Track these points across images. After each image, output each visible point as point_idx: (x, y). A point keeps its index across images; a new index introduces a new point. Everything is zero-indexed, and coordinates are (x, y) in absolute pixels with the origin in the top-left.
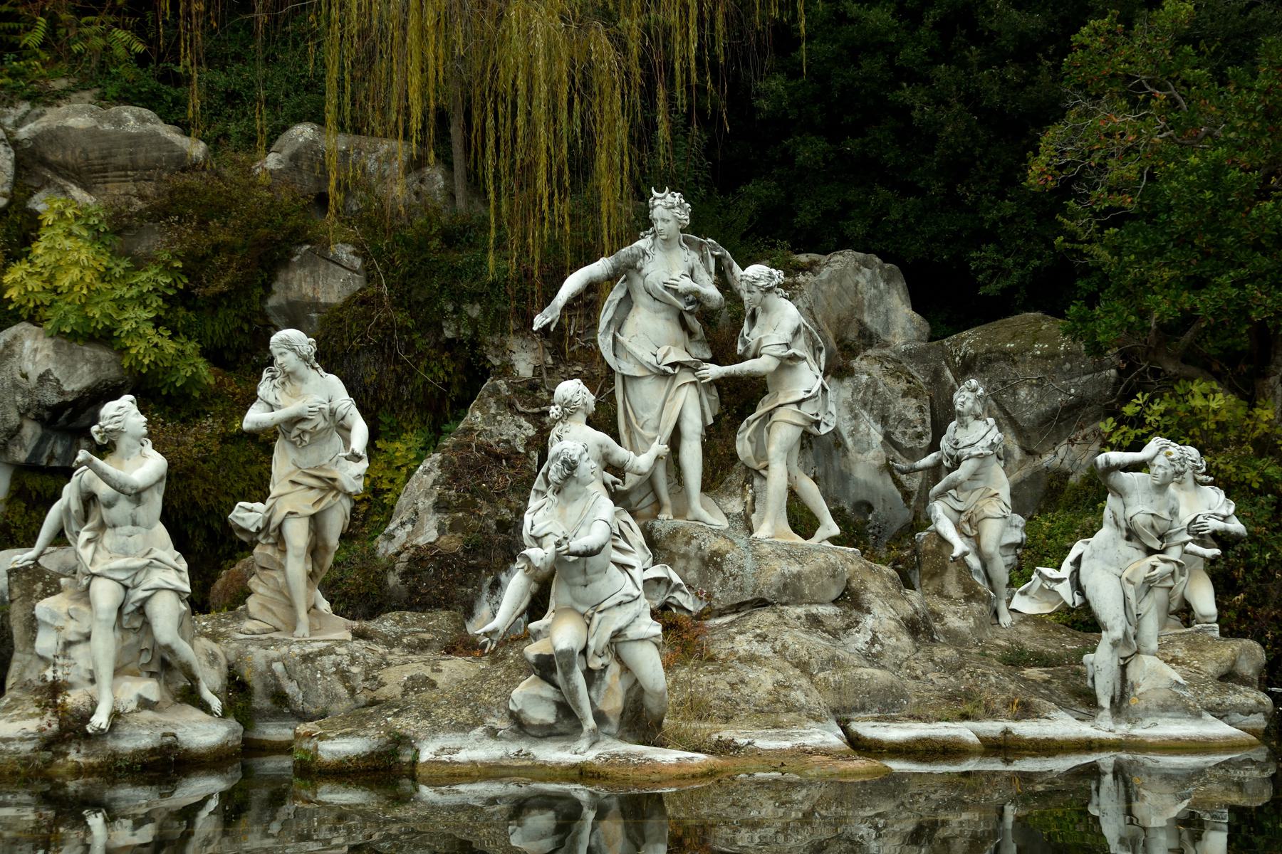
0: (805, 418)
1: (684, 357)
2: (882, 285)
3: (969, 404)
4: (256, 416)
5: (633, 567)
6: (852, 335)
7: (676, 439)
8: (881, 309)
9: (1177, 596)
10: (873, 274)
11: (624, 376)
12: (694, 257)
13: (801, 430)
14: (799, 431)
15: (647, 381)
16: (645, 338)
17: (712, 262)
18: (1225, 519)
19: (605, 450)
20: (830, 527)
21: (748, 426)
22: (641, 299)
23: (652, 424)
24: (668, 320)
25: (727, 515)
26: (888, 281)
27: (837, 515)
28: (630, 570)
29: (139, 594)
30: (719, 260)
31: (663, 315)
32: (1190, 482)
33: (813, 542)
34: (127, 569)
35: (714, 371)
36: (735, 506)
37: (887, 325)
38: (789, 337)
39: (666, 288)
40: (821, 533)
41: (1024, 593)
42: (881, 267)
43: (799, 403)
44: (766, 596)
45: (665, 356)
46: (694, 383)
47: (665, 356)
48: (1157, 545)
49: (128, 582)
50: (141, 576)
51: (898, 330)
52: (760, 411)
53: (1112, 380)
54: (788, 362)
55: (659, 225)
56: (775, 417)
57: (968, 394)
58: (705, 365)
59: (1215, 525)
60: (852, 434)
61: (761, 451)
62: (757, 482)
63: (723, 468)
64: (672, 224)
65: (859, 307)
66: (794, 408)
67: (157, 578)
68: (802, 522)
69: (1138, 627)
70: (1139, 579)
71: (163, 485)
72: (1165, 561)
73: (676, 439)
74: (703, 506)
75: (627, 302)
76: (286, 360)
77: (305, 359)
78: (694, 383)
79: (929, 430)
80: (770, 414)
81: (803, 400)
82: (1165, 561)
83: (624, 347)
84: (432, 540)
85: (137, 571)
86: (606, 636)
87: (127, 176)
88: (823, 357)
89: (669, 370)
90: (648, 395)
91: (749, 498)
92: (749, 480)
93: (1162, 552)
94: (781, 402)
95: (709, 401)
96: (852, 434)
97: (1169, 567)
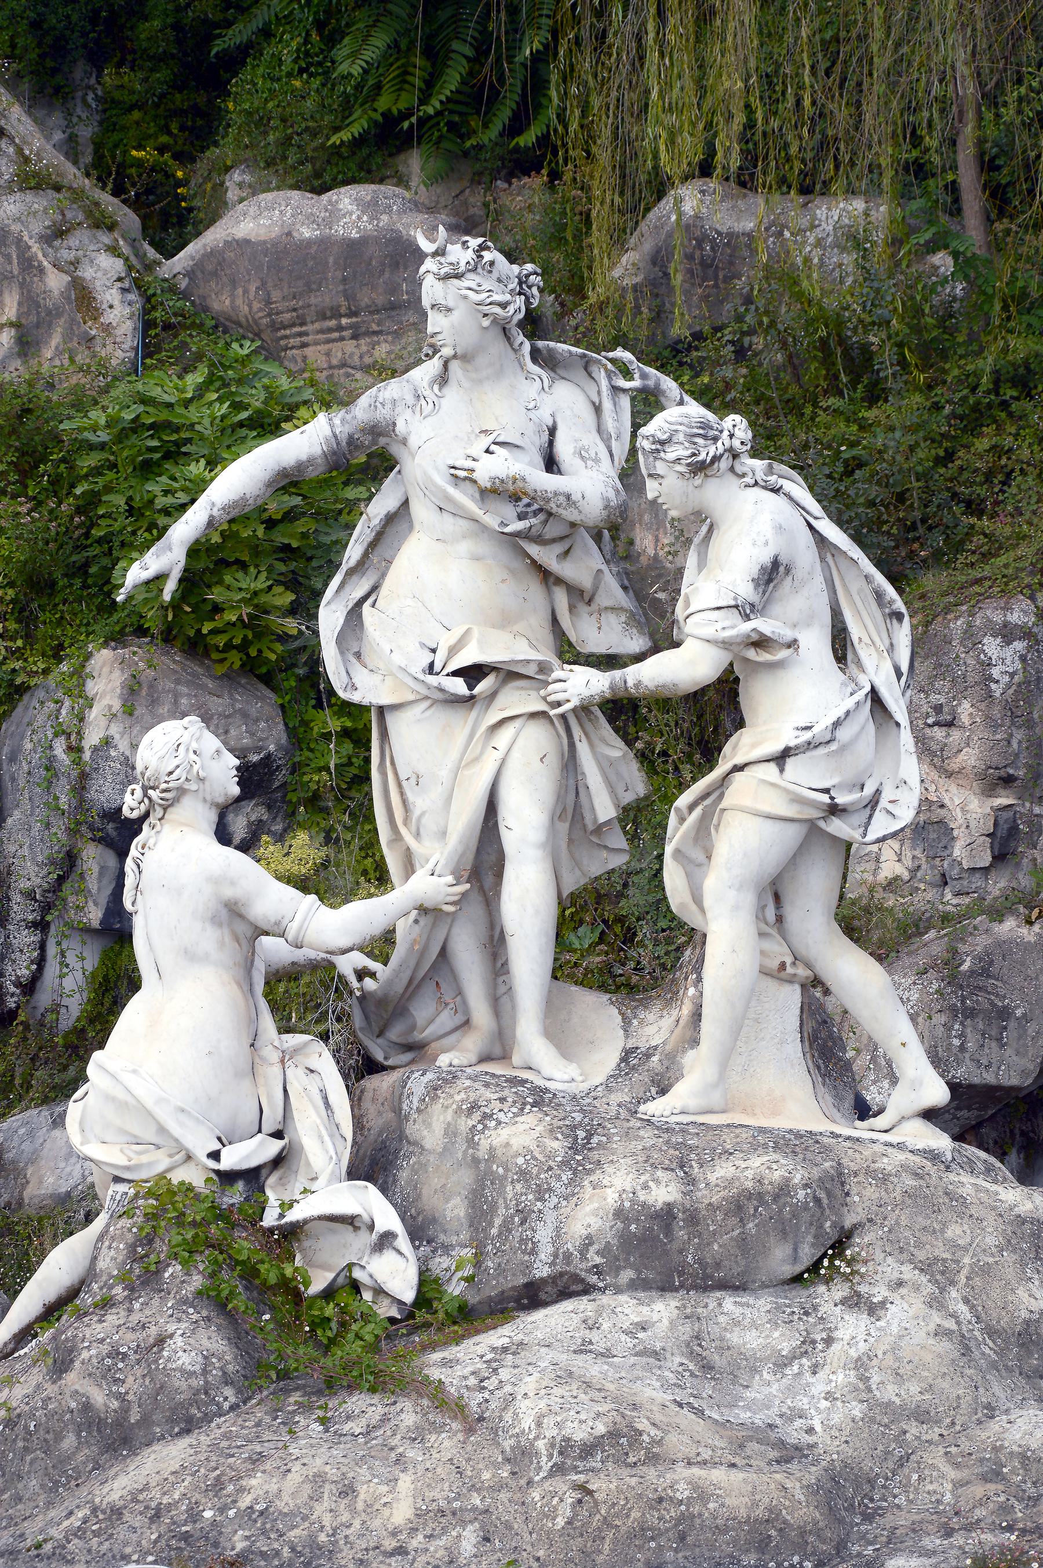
0: (798, 800)
7: (484, 863)
11: (381, 710)
14: (793, 834)
16: (413, 612)
19: (228, 893)
21: (682, 820)
24: (476, 558)
31: (465, 547)
35: (583, 683)
38: (746, 591)
43: (781, 758)
44: (579, 1267)
47: (453, 651)
54: (751, 654)
55: (435, 322)
63: (622, 939)
66: (772, 767)
73: (484, 863)
74: (557, 1031)
84: (74, 1110)
87: (340, 328)
89: (459, 686)
94: (739, 760)
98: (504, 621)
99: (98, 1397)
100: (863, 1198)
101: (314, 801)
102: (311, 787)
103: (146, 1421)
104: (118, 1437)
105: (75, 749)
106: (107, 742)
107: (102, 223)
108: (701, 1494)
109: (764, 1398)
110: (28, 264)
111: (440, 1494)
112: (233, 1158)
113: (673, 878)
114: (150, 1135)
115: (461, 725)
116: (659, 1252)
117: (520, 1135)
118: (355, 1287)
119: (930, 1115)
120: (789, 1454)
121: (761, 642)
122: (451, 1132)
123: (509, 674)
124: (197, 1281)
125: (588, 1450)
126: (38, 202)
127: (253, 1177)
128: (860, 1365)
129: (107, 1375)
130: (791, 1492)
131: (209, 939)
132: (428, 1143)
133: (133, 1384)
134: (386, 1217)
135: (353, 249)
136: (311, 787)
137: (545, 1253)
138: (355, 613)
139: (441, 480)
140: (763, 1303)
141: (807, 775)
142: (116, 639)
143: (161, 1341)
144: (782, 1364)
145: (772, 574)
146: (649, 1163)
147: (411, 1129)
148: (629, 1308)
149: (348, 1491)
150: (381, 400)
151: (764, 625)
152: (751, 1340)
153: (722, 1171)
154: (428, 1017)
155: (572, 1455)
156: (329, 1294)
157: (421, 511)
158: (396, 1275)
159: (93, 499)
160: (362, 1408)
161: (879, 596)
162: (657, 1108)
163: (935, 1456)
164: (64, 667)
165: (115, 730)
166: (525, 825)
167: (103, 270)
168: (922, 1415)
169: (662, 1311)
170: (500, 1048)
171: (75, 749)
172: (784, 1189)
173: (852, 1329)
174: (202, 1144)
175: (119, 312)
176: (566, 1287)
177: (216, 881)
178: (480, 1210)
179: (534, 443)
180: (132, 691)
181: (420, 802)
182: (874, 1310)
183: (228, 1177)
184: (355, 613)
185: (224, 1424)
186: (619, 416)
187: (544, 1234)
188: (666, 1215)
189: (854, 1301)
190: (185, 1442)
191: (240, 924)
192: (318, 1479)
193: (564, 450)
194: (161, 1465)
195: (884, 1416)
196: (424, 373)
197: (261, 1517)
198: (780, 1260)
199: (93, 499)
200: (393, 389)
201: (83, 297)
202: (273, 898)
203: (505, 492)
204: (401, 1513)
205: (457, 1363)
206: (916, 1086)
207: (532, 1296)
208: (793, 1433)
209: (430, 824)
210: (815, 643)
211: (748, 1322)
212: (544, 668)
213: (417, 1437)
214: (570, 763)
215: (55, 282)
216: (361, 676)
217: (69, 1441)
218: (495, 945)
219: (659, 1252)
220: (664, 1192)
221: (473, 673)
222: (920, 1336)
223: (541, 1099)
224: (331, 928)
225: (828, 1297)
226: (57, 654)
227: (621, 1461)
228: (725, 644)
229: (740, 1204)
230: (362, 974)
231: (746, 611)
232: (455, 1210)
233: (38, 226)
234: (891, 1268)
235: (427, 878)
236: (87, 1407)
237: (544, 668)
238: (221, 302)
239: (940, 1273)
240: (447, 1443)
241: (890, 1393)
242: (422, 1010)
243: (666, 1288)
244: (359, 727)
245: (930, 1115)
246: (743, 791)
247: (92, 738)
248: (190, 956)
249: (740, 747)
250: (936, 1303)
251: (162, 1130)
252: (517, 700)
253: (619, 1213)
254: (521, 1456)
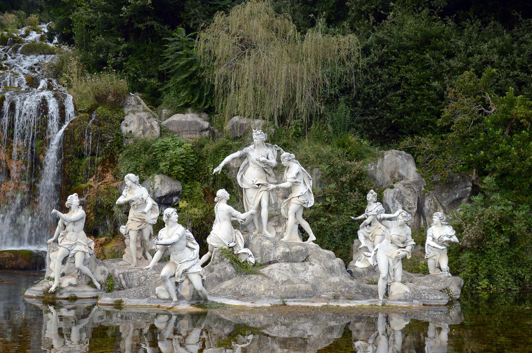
0: (301, 202)
2: (405, 161)
3: (371, 198)
4: (121, 200)
6: (396, 176)
7: (259, 207)
8: (406, 168)
9: (437, 262)
10: (402, 157)
14: (300, 206)
15: (249, 190)
18: (451, 237)
19: (230, 211)
20: (312, 237)
23: (252, 203)
26: (407, 160)
27: (316, 234)
29: (72, 252)
31: (257, 169)
32: (440, 224)
33: (307, 242)
34: (69, 245)
35: (272, 186)
37: (408, 173)
38: (295, 176)
40: (309, 239)
41: (359, 261)
42: (405, 156)
43: (298, 197)
44: (277, 259)
48: (401, 245)
49: (69, 249)
50: (73, 247)
51: (412, 175)
53: (470, 191)
55: (255, 140)
57: (370, 194)
59: (446, 239)
60: (392, 208)
63: (277, 218)
65: (396, 168)
66: (297, 198)
67: (77, 248)
68: (305, 237)
69: (394, 273)
70: (394, 257)
71: (84, 220)
72: (404, 251)
73: (259, 207)
76: (128, 183)
77: (135, 183)
79: (416, 206)
80: (290, 200)
82: (404, 251)
85: (72, 245)
86: (181, 271)
88: (311, 182)
89: (257, 186)
93: (405, 247)
95: (273, 196)
96: (392, 208)
97: (404, 253)
98: (261, 178)
99: (218, 275)
100: (310, 252)
101: (186, 197)
102: (237, 199)
103: (224, 278)
104: (221, 280)
105: (153, 189)
106: (158, 188)
107: (155, 117)
108: (300, 287)
109: (302, 275)
110: (144, 122)
111: (267, 287)
112: (231, 245)
113: (283, 211)
114: (220, 242)
115: (256, 191)
116: (287, 258)
117: (267, 243)
118: (246, 261)
119: (313, 241)
120: (306, 283)
121: (296, 182)
122: (257, 242)
123: (263, 185)
124: (229, 261)
125: (285, 282)
126: (146, 114)
127: (232, 247)
128: (312, 272)
129: (219, 272)
130: (308, 287)
131: (227, 217)
132: (254, 243)
133: (222, 273)
134: (250, 253)
135: (190, 122)
136: (237, 199)
137: (272, 257)
138: (242, 176)
139: (255, 160)
140: (299, 264)
141: (301, 199)
142: (158, 174)
143: (225, 268)
144: (303, 272)
145: (298, 174)
146: (284, 246)
147: (251, 242)
148: (284, 265)
149: (255, 287)
150: (245, 150)
151: (297, 180)
152: (299, 269)
153: (294, 248)
154: (250, 228)
155: (284, 282)
156: (244, 262)
157: (251, 164)
158: (252, 260)
159: (155, 155)
160: (254, 277)
161: (308, 177)
162: (282, 240)
163: (323, 283)
164: (151, 177)
165: (159, 186)
166: (265, 204)
167: (155, 123)
168: (321, 278)
169: (288, 265)
170: (260, 232)
171: (153, 189)
172: (302, 250)
173: (311, 267)
174: (227, 244)
175: (157, 129)
176: (275, 262)
177: (228, 210)
178: (262, 252)
179: (266, 156)
180: (162, 181)
181: (250, 201)
182: (313, 265)
183: (230, 247)
184: (242, 176)
185: (234, 279)
186: (276, 153)
187: (272, 255)
188: (288, 253)
189: (310, 264)
190: (230, 281)
191: (231, 215)
192: (251, 285)
193: (270, 157)
194: (227, 283)
195: (316, 278)
196: (252, 146)
197: (244, 290)
198: (302, 259)
199: (155, 155)
200: (248, 148)
201: (152, 127)
202: (235, 212)
203: (263, 162)
204: (263, 289)
205: (265, 270)
206: (312, 238)
207: (270, 263)
208: (306, 280)
209: (252, 203)
210: (302, 182)
211: (298, 266)
212: (267, 184)
213: (262, 280)
214: (269, 196)
215: (148, 125)
216: (243, 184)
217: (214, 280)
218: (260, 218)
219: (287, 258)
220: (288, 250)
221: (258, 185)
222: (319, 268)
223: (268, 238)
224: (241, 216)
225: (307, 263)
226: (149, 175)
227: (289, 283)
228: (292, 182)
229: (297, 252)
230: (241, 222)
231: (295, 178)
232: (258, 252)
233: (146, 117)
234: (314, 260)
235: (252, 210)
236: (216, 276)
237: (267, 184)
238: (171, 128)
239: (320, 260)
240: (266, 281)
241: (316, 275)
242: (248, 227)
243: (288, 262)
244: (241, 189)
245: (313, 241)
246: (293, 201)
247: (156, 187)
248: (225, 219)
249: (294, 195)
250: (320, 264)
251: (222, 241)
252: (264, 188)
253: (282, 253)
254: (277, 282)
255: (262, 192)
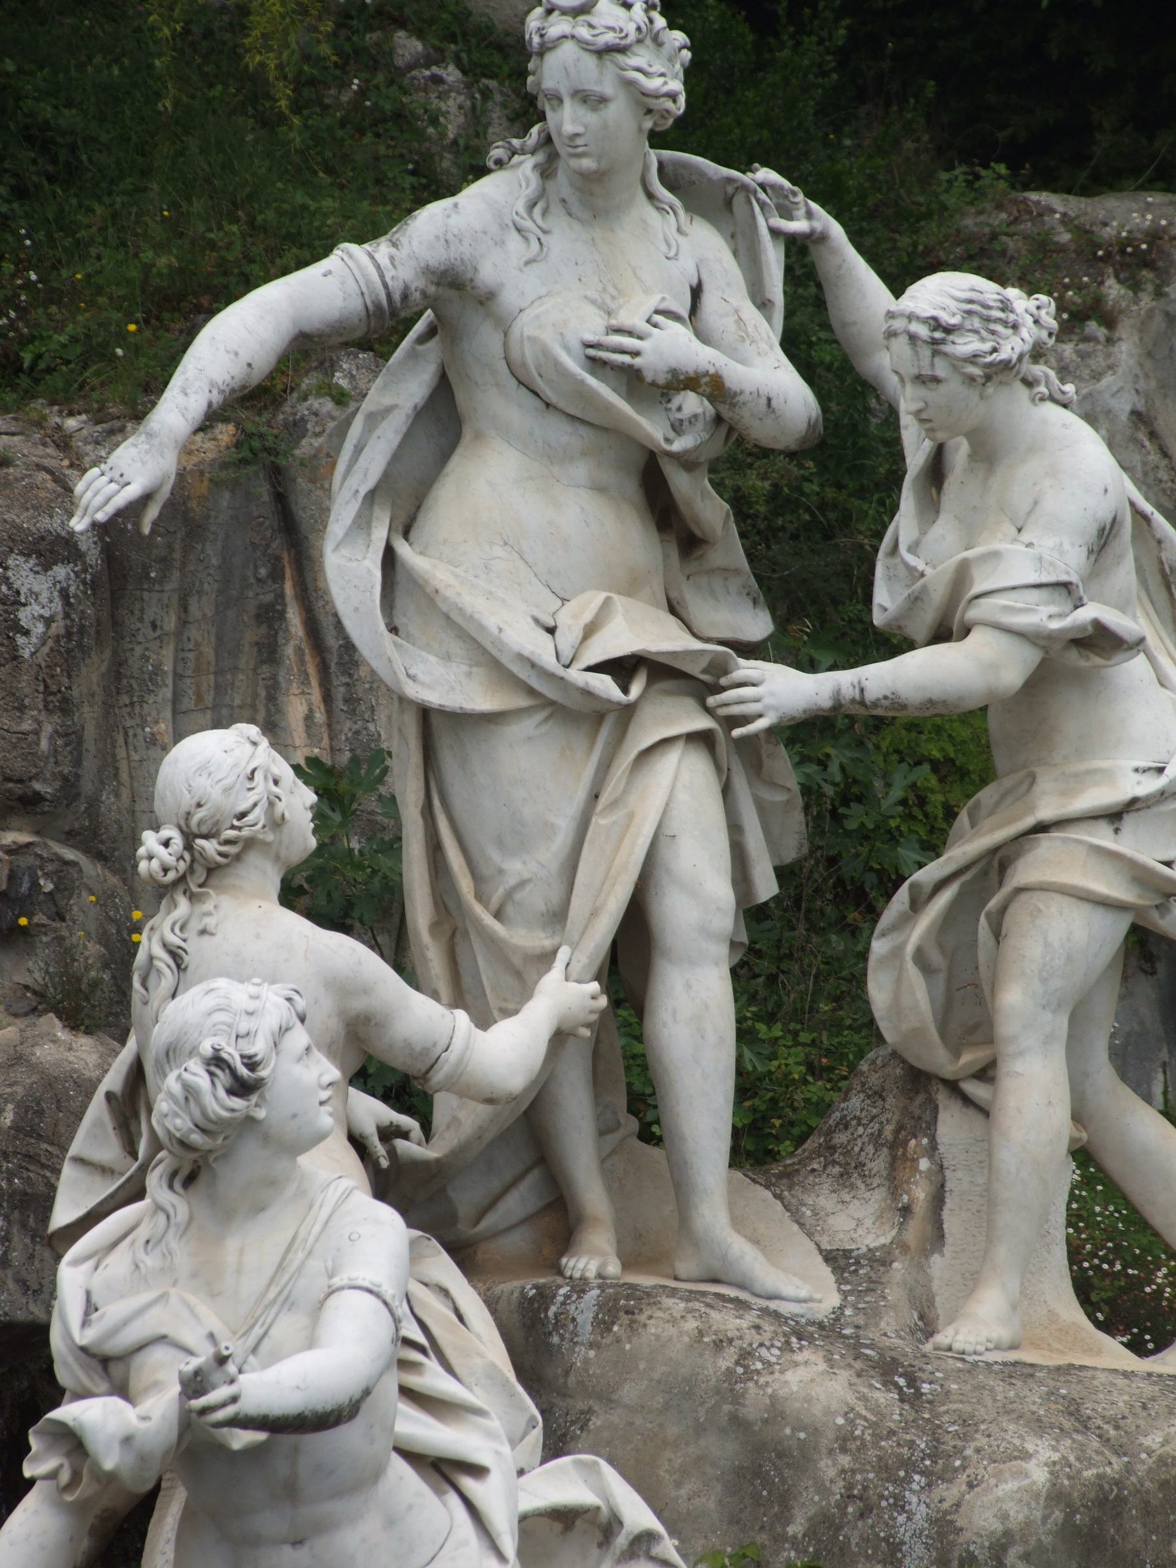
0: (1140, 875)
1: (662, 637)
5: (478, 1471)
7: (630, 961)
11: (426, 714)
12: (704, 246)
13: (1120, 926)
14: (1115, 929)
16: (510, 568)
17: (774, 259)
19: (358, 1005)
21: (917, 904)
22: (494, 404)
23: (538, 899)
24: (599, 489)
25: (830, 1257)
28: (468, 1483)
30: (801, 253)
35: (782, 690)
36: (859, 1220)
38: (1070, 562)
39: (596, 365)
43: (1115, 816)
45: (590, 631)
46: (702, 739)
47: (590, 631)
52: (965, 847)
54: (1074, 657)
55: (567, 119)
56: (1025, 872)
58: (747, 668)
61: (968, 1009)
62: (952, 1125)
64: (619, 111)
73: (630, 961)
74: (737, 1223)
75: (443, 422)
78: (702, 739)
80: (998, 862)
81: (1133, 805)
83: (428, 597)
89: (605, 685)
90: (527, 783)
91: (920, 1193)
92: (927, 1125)
94: (1046, 811)
95: (762, 808)
139: (573, 365)
150: (433, 230)
181: (515, 868)
253: (1056, 1496)
255: (672, 759)
